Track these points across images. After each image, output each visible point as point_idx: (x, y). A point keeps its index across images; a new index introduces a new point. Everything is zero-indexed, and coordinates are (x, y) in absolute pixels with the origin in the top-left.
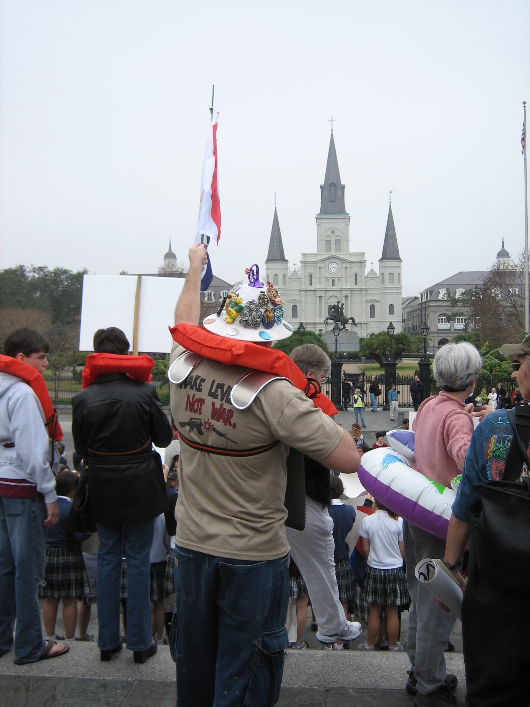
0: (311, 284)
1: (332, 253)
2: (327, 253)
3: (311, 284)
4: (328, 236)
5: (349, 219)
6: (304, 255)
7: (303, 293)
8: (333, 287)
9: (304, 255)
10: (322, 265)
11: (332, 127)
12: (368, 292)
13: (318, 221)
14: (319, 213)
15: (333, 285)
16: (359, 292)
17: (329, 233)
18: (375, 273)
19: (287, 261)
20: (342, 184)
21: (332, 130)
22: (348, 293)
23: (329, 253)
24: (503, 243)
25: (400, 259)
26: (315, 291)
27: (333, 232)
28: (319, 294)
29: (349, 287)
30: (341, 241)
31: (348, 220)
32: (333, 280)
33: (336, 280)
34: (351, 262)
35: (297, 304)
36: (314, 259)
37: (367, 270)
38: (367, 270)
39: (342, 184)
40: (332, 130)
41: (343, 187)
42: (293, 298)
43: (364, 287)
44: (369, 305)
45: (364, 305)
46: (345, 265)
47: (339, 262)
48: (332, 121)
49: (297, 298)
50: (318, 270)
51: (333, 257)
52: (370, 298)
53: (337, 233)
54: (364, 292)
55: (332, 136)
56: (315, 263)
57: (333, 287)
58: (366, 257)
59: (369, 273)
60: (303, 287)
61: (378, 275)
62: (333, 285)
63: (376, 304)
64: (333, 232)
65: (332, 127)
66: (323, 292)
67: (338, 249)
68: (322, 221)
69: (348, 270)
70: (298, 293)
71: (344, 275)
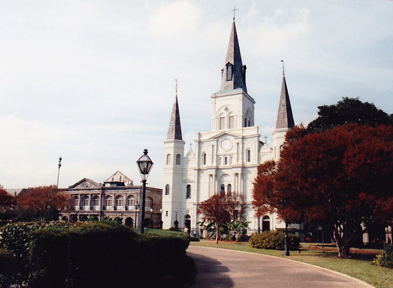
1: (226, 130)
4: (221, 114)
10: (215, 143)
11: (234, 16)
17: (223, 110)
20: (243, 64)
21: (234, 19)
22: (239, 171)
30: (235, 117)
33: (228, 157)
34: (243, 138)
39: (243, 64)
40: (234, 19)
41: (245, 67)
47: (232, 138)
48: (235, 10)
55: (234, 23)
57: (226, 165)
64: (226, 109)
65: (234, 16)
69: (240, 145)
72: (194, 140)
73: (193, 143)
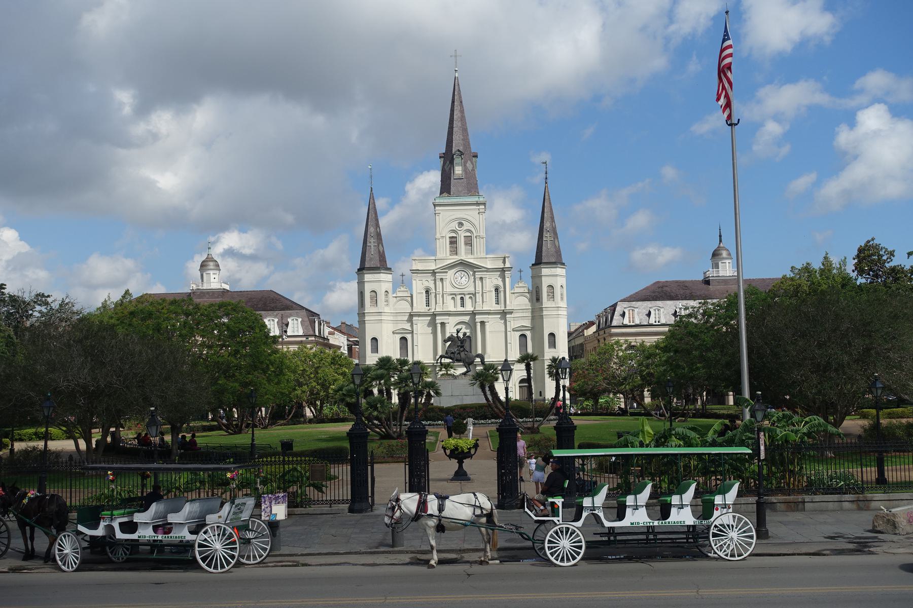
0: (428, 304)
4: (453, 231)
8: (462, 309)
15: (463, 305)
17: (455, 226)
19: (390, 269)
23: (455, 257)
24: (720, 236)
25: (563, 264)
27: (461, 224)
29: (486, 308)
32: (462, 299)
33: (467, 298)
34: (488, 270)
35: (409, 337)
42: (401, 326)
53: (467, 226)
56: (434, 273)
62: (463, 305)
64: (461, 224)
71: (479, 288)
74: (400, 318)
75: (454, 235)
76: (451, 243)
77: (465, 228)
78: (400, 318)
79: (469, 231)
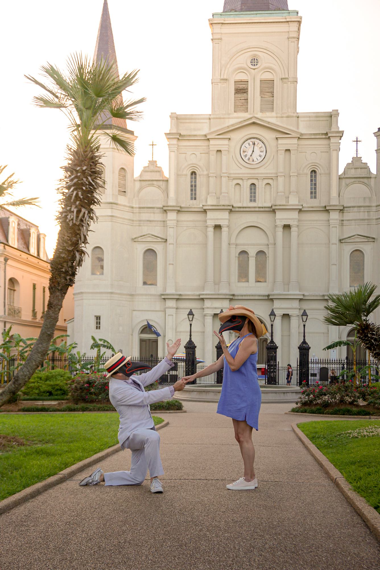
2: (235, 115)
3: (194, 197)
4: (241, 70)
5: (299, 22)
6: (176, 119)
7: (172, 216)
8: (253, 204)
9: (176, 119)
12: (347, 216)
13: (218, 29)
14: (220, 10)
15: (253, 198)
16: (323, 216)
18: (365, 167)
26: (205, 211)
27: (254, 61)
28: (213, 218)
29: (293, 201)
31: (294, 27)
33: (260, 185)
35: (158, 248)
36: (205, 130)
37: (344, 158)
38: (344, 158)
42: (145, 230)
43: (334, 202)
44: (348, 249)
45: (334, 248)
46: (285, 143)
47: (268, 136)
49: (157, 231)
50: (213, 157)
51: (254, 123)
52: (350, 230)
53: (265, 60)
54: (334, 216)
57: (253, 204)
58: (342, 124)
59: (348, 167)
60: (172, 203)
61: (374, 170)
62: (253, 198)
63: (367, 249)
66: (225, 215)
67: (268, 104)
68: (226, 29)
70: (158, 216)
72: (166, 134)
73: (163, 144)
74: (145, 216)
75: (242, 77)
76: (238, 91)
77: (262, 64)
78: (145, 216)
79: (268, 69)
